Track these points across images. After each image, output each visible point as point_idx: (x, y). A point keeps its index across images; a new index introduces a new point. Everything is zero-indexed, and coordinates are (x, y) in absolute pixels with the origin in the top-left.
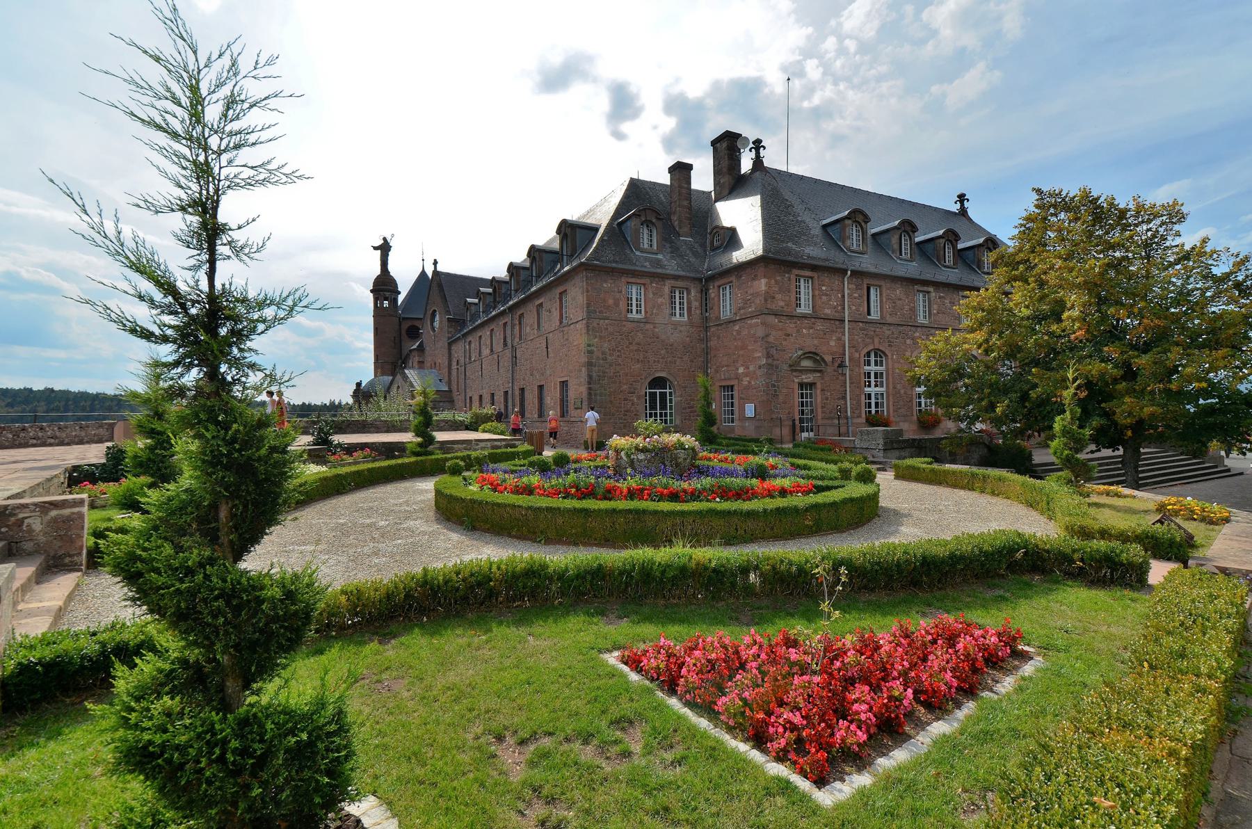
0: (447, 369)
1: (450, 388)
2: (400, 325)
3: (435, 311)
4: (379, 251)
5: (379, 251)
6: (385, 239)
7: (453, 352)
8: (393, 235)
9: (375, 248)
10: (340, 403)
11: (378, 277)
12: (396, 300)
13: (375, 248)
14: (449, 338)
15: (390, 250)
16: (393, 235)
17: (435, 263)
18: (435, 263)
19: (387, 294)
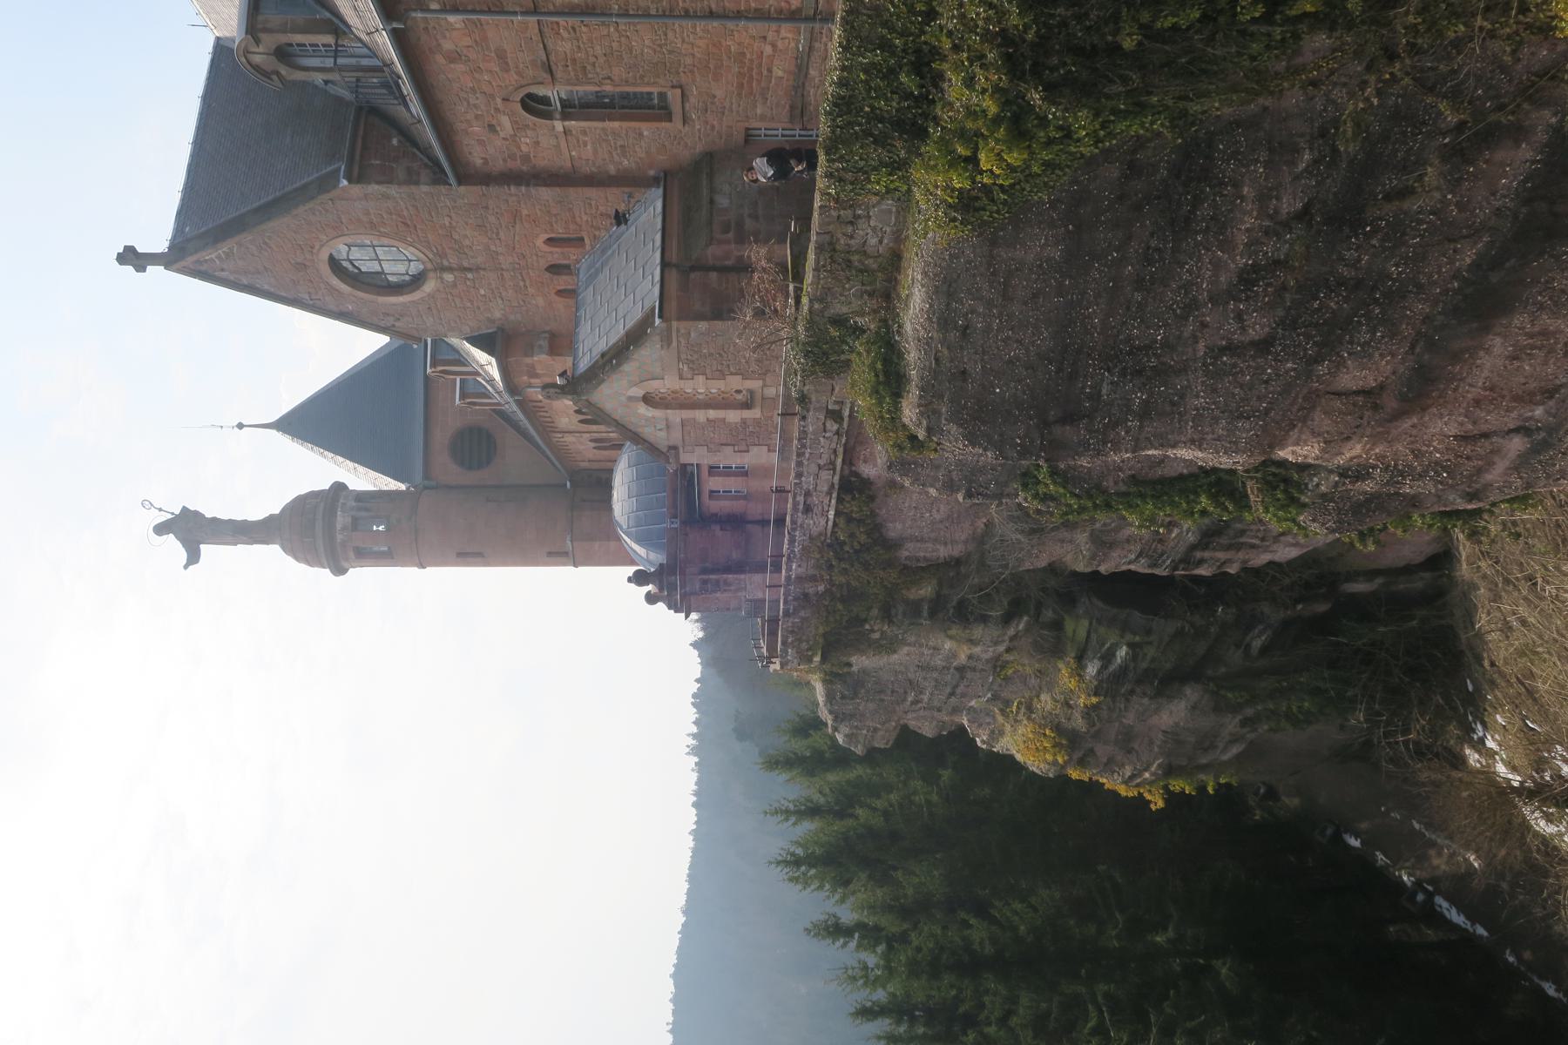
0: (572, 192)
1: (655, 181)
2: (449, 487)
3: (334, 263)
4: (202, 546)
5: (202, 546)
6: (161, 529)
7: (499, 165)
8: (147, 504)
9: (193, 557)
10: (694, 736)
11: (291, 550)
12: (362, 497)
13: (193, 557)
14: (439, 178)
15: (196, 513)
16: (147, 504)
17: (132, 257)
18: (132, 257)
19: (341, 520)
